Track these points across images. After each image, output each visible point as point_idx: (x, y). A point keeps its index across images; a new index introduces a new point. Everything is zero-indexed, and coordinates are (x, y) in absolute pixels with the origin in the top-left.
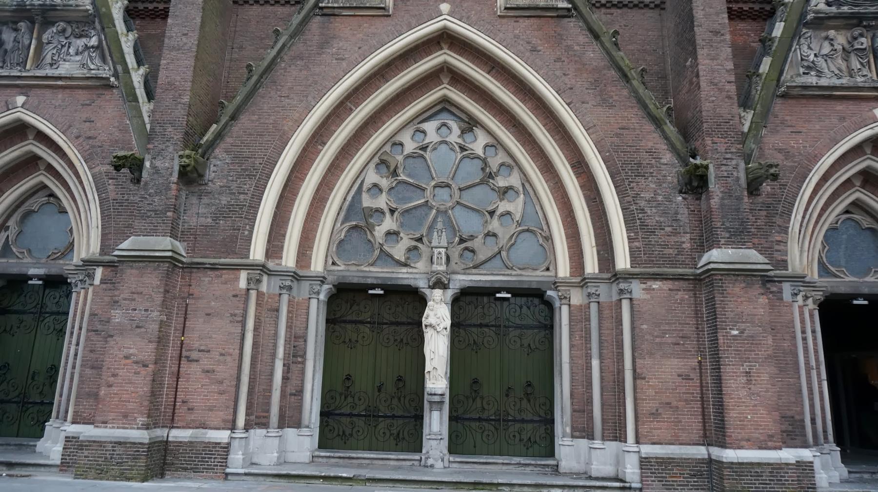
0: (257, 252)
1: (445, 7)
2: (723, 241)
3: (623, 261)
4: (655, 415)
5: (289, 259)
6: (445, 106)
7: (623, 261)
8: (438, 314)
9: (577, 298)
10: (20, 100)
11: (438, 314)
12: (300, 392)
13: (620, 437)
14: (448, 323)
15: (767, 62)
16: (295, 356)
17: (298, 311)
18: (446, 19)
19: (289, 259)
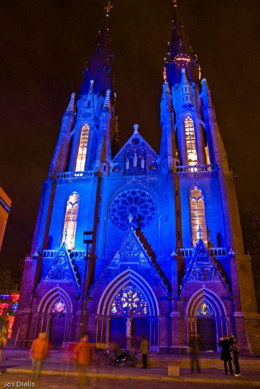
0: (98, 312)
1: (129, 267)
2: (174, 310)
3: (158, 314)
4: (162, 340)
5: (103, 313)
6: (130, 284)
7: (158, 314)
8: (129, 324)
9: (153, 320)
10: (58, 285)
11: (129, 324)
12: (105, 337)
13: (157, 345)
14: (130, 325)
15: (185, 276)
16: (105, 330)
17: (105, 323)
18: (129, 270)
19: (103, 313)
